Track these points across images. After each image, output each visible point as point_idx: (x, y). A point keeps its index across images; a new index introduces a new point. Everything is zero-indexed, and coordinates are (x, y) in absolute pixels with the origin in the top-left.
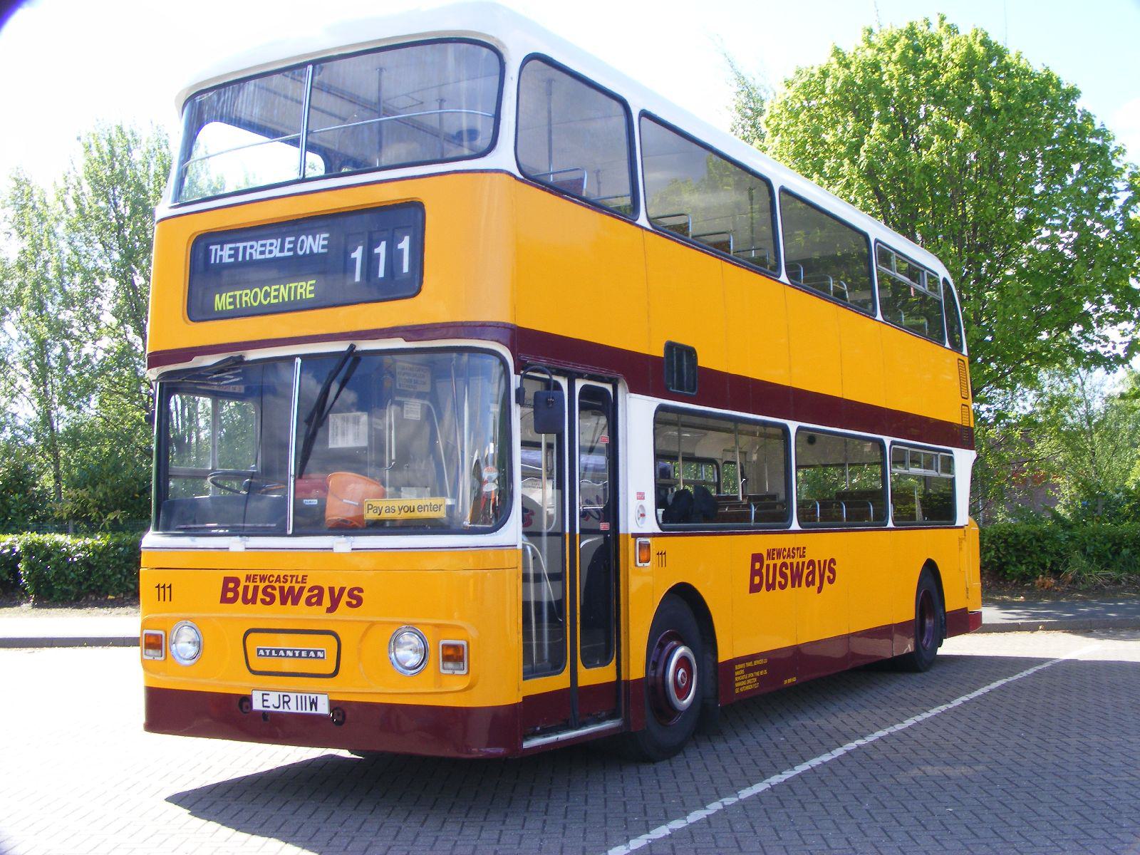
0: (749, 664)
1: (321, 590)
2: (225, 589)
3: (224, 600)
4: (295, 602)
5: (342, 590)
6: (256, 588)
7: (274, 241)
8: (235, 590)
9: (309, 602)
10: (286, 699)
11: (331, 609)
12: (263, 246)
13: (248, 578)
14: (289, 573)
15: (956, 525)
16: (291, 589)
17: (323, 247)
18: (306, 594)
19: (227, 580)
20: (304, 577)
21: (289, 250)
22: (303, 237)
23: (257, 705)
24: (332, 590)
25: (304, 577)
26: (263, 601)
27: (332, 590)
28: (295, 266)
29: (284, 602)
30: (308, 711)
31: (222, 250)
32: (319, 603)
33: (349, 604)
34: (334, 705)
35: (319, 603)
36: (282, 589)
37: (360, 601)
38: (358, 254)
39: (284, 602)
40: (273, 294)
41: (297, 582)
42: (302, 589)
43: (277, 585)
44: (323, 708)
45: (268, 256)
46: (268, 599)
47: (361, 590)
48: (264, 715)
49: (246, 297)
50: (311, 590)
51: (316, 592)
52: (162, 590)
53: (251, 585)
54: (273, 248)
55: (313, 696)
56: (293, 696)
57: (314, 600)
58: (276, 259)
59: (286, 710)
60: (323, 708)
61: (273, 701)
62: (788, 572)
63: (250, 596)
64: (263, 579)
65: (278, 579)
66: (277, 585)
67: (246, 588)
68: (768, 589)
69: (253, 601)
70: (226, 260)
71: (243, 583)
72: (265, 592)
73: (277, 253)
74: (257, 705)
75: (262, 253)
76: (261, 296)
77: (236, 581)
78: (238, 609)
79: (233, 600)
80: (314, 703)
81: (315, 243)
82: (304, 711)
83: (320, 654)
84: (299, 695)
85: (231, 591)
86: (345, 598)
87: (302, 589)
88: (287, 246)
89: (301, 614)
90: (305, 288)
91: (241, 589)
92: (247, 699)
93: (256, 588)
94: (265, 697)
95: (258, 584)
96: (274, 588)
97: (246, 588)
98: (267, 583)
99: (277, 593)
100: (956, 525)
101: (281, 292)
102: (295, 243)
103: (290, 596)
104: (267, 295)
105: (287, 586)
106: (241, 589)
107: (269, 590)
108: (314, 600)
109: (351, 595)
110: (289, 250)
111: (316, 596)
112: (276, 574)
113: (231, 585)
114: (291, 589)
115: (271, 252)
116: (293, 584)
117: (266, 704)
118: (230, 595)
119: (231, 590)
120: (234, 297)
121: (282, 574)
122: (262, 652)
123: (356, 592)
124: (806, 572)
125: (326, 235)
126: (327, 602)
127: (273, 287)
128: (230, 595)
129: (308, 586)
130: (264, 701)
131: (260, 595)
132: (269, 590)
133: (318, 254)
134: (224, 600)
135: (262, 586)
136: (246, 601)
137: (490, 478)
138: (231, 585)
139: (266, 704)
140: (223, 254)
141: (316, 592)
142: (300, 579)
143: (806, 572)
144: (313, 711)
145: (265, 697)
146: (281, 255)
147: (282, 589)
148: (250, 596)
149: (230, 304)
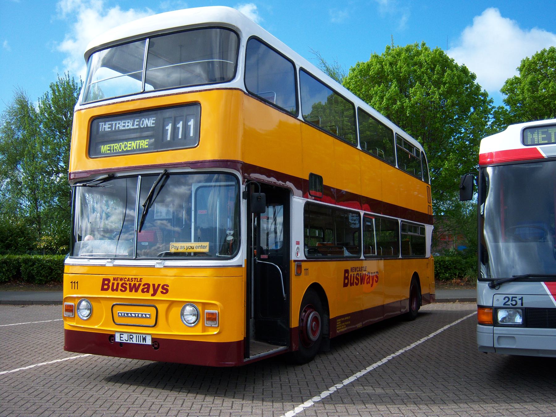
0: (343, 319)
1: (149, 285)
2: (103, 284)
3: (103, 289)
5: (159, 285)
6: (118, 284)
7: (130, 121)
8: (108, 285)
9: (143, 291)
10: (131, 337)
12: (124, 123)
13: (114, 279)
14: (133, 277)
16: (135, 284)
17: (153, 123)
18: (141, 287)
19: (104, 280)
20: (141, 279)
21: (137, 125)
22: (143, 119)
23: (118, 339)
24: (154, 285)
25: (141, 279)
26: (121, 290)
27: (154, 285)
28: (141, 133)
29: (131, 290)
30: (142, 343)
31: (105, 125)
32: (148, 291)
33: (162, 292)
34: (154, 340)
35: (148, 291)
36: (130, 284)
37: (167, 291)
38: (169, 127)
40: (129, 145)
41: (137, 281)
42: (140, 285)
43: (128, 283)
44: (149, 342)
45: (126, 128)
46: (123, 289)
47: (168, 286)
48: (121, 344)
49: (116, 146)
50: (144, 285)
51: (146, 286)
52: (73, 284)
53: (116, 282)
54: (129, 124)
55: (144, 336)
56: (134, 336)
57: (145, 290)
58: (130, 129)
59: (131, 342)
60: (149, 342)
61: (125, 337)
62: (359, 278)
63: (115, 288)
64: (121, 279)
65: (128, 280)
66: (128, 283)
67: (113, 284)
68: (351, 286)
69: (117, 290)
70: (107, 130)
71: (112, 281)
73: (131, 127)
74: (118, 339)
75: (124, 126)
76: (123, 146)
77: (109, 280)
78: (109, 294)
79: (107, 289)
80: (144, 339)
81: (149, 122)
82: (140, 343)
83: (148, 316)
84: (137, 335)
85: (106, 285)
86: (160, 289)
87: (140, 285)
88: (136, 123)
89: (139, 296)
90: (144, 143)
91: (111, 284)
92: (112, 337)
93: (118, 284)
94: (122, 336)
96: (126, 284)
97: (113, 284)
98: (123, 282)
99: (128, 286)
101: (133, 145)
102: (139, 122)
103: (134, 288)
104: (126, 146)
106: (111, 284)
107: (124, 285)
108: (145, 290)
109: (163, 288)
110: (137, 125)
112: (127, 277)
113: (106, 282)
114: (135, 284)
115: (128, 126)
116: (136, 282)
117: (122, 339)
118: (106, 287)
119: (106, 284)
120: (110, 147)
121: (130, 277)
122: (120, 314)
123: (165, 287)
124: (366, 277)
125: (155, 118)
126: (151, 291)
127: (129, 142)
128: (106, 287)
129: (143, 283)
130: (121, 337)
131: (120, 287)
132: (124, 285)
133: (150, 127)
134: (103, 289)
135: (121, 283)
137: (230, 233)
138: (106, 282)
139: (122, 339)
140: (105, 127)
141: (146, 286)
142: (139, 280)
143: (366, 277)
144: (144, 343)
145: (122, 336)
146: (133, 127)
148: (115, 288)
149: (108, 150)
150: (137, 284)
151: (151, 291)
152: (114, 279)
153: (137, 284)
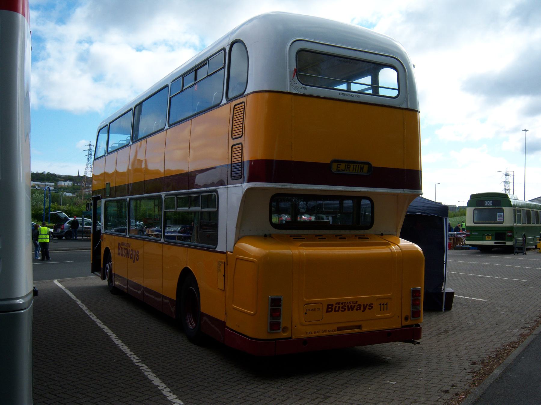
1: (360, 305)
2: (328, 308)
3: (327, 311)
4: (352, 310)
5: (367, 305)
6: (339, 307)
11: (363, 311)
13: (336, 304)
15: (217, 249)
16: (351, 306)
18: (356, 307)
24: (364, 305)
26: (342, 311)
27: (364, 305)
29: (349, 310)
32: (360, 309)
33: (369, 309)
35: (360, 309)
36: (348, 306)
37: (372, 307)
39: (349, 310)
42: (354, 306)
47: (372, 304)
53: (337, 306)
63: (337, 309)
64: (342, 303)
67: (336, 307)
69: (338, 311)
72: (342, 308)
77: (332, 305)
86: (368, 307)
87: (354, 306)
91: (334, 308)
93: (339, 307)
97: (336, 307)
99: (346, 308)
100: (217, 249)
103: (351, 308)
105: (350, 305)
106: (334, 308)
109: (369, 306)
111: (359, 308)
113: (330, 307)
114: (351, 306)
118: (330, 310)
126: (362, 309)
128: (330, 310)
131: (341, 309)
135: (341, 306)
136: (335, 311)
138: (330, 307)
147: (348, 306)
148: (337, 309)
151: (362, 309)
152: (336, 304)
153: (353, 305)
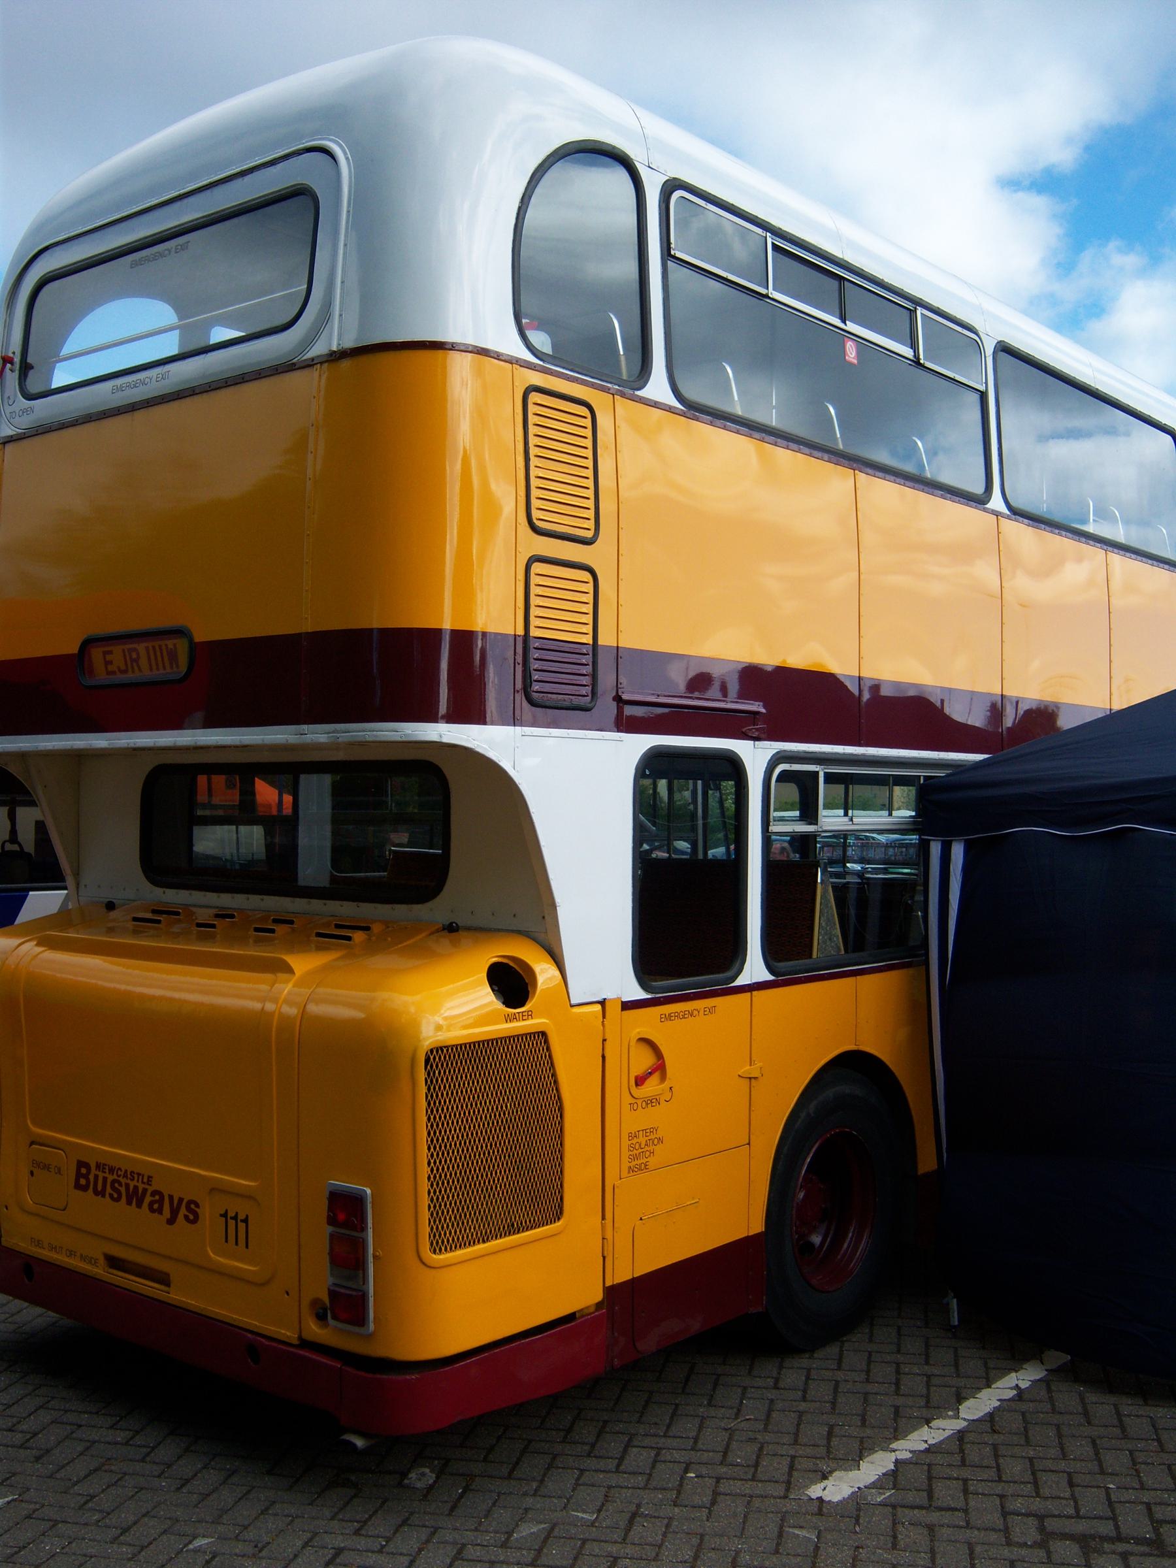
5: (181, 1200)
6: (105, 1179)
16: (136, 1187)
18: (148, 1199)
27: (171, 1197)
36: (127, 1185)
42: (145, 1190)
50: (154, 1193)
51: (157, 1197)
67: (96, 1177)
95: (107, 1175)
97: (96, 1177)
99: (123, 1190)
106: (91, 1177)
114: (136, 1187)
135: (110, 1178)
141: (157, 1197)
150: (141, 1187)
